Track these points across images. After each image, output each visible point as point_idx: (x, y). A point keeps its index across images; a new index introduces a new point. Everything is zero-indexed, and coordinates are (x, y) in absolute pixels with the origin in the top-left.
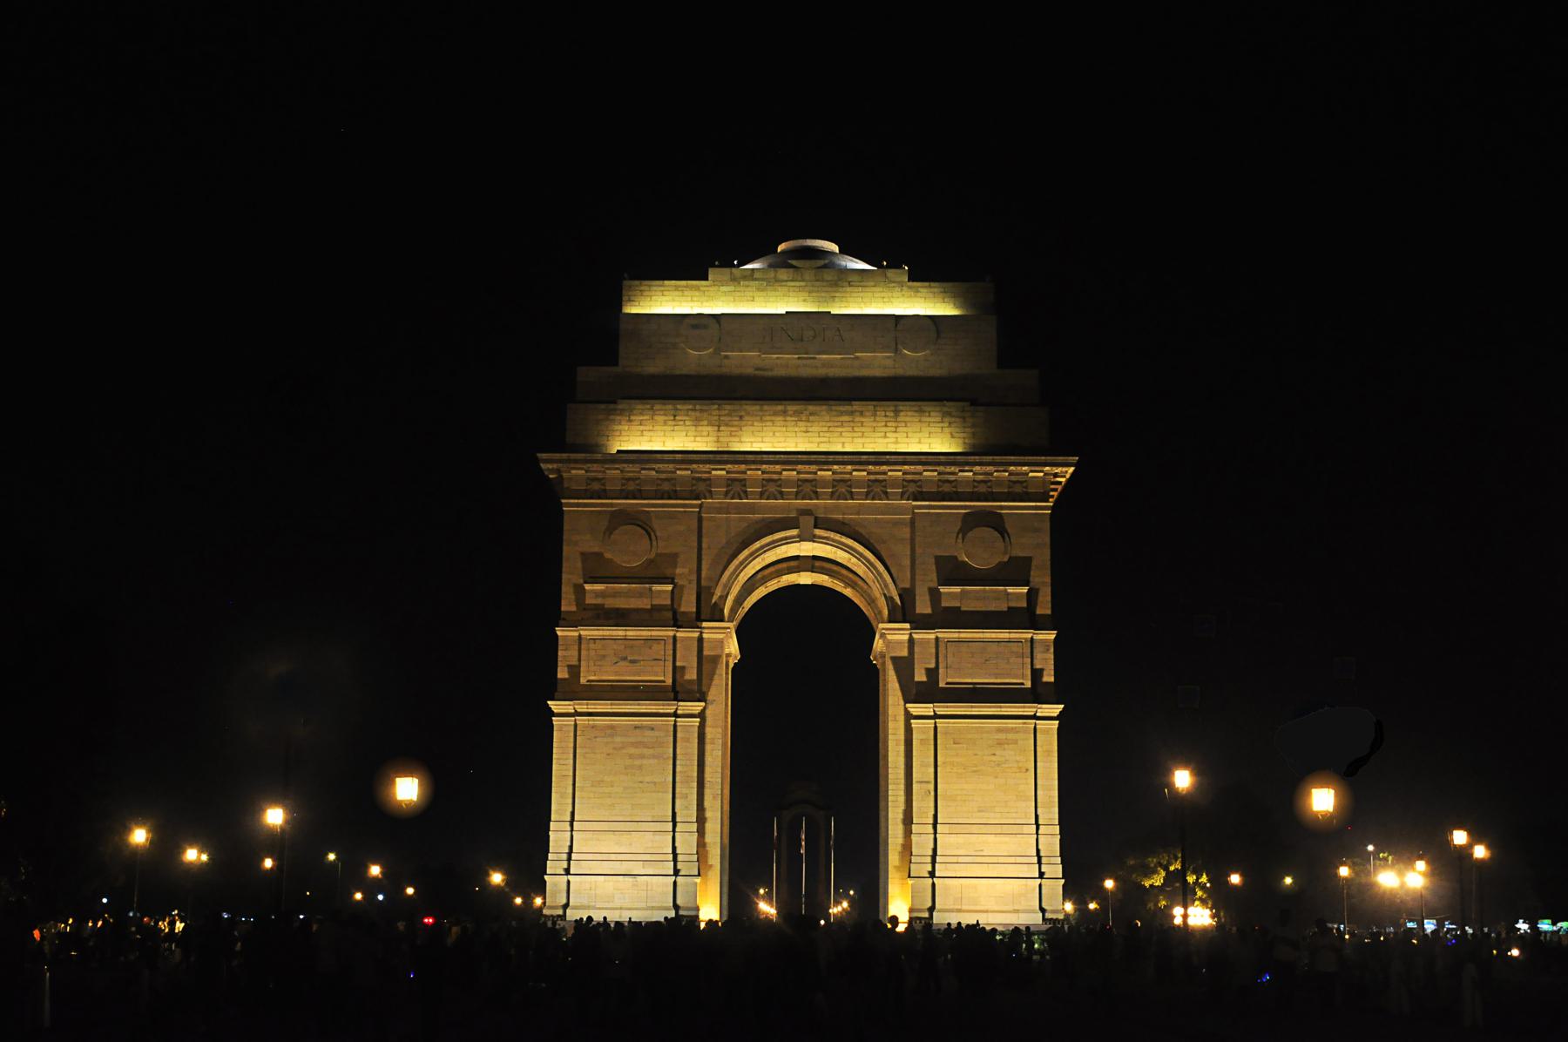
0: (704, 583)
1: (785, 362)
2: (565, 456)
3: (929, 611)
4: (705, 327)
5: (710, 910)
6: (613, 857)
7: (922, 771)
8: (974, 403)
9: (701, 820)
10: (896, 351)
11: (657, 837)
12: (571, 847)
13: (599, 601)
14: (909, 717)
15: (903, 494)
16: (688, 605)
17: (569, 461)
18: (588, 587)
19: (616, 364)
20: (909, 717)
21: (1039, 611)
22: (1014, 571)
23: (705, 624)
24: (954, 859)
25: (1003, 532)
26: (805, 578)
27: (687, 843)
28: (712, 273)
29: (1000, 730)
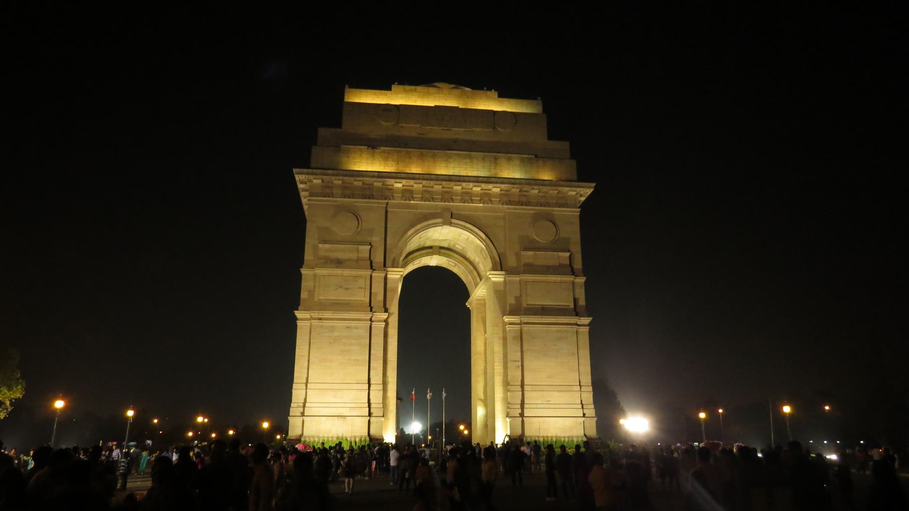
1: (435, 132)
2: (310, 171)
5: (390, 438)
6: (332, 405)
8: (536, 156)
9: (385, 383)
10: (494, 128)
12: (305, 399)
13: (327, 254)
16: (378, 258)
17: (312, 174)
18: (321, 246)
20: (504, 324)
21: (575, 267)
23: (389, 269)
26: (434, 261)
27: (376, 397)
28: (393, 86)
29: (557, 331)
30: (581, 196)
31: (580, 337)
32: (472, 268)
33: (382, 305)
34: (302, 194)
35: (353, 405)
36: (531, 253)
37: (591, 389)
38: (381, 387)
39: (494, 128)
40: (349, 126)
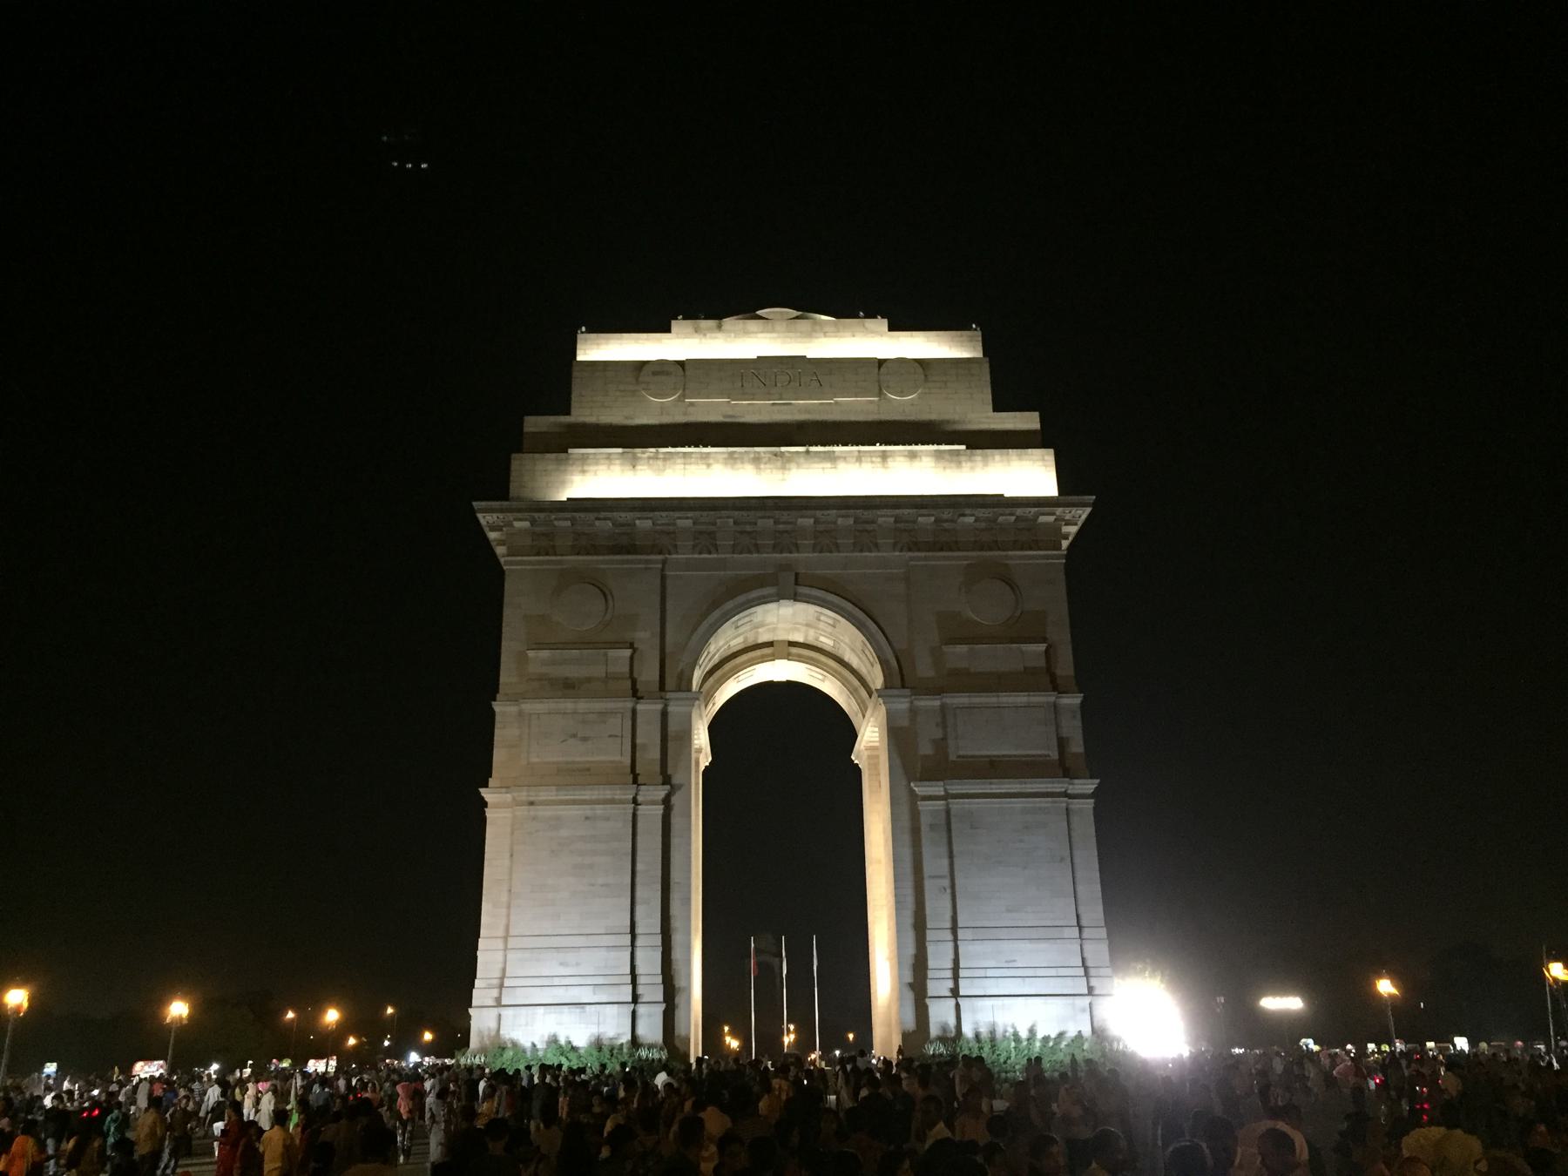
0: (668, 650)
3: (931, 673)
4: (668, 374)
6: (556, 981)
7: (935, 864)
10: (880, 394)
11: (613, 954)
12: (504, 970)
14: (913, 797)
15: (895, 544)
16: (648, 673)
18: (531, 654)
19: (567, 411)
20: (913, 797)
21: (1059, 672)
22: (1023, 629)
23: (669, 695)
24: (981, 973)
25: (1010, 583)
30: (1068, 523)
31: (1075, 819)
32: (856, 683)
33: (657, 768)
34: (500, 550)
35: (600, 980)
36: (962, 649)
37: (1103, 933)
38: (658, 940)
39: (880, 394)
40: (584, 412)
